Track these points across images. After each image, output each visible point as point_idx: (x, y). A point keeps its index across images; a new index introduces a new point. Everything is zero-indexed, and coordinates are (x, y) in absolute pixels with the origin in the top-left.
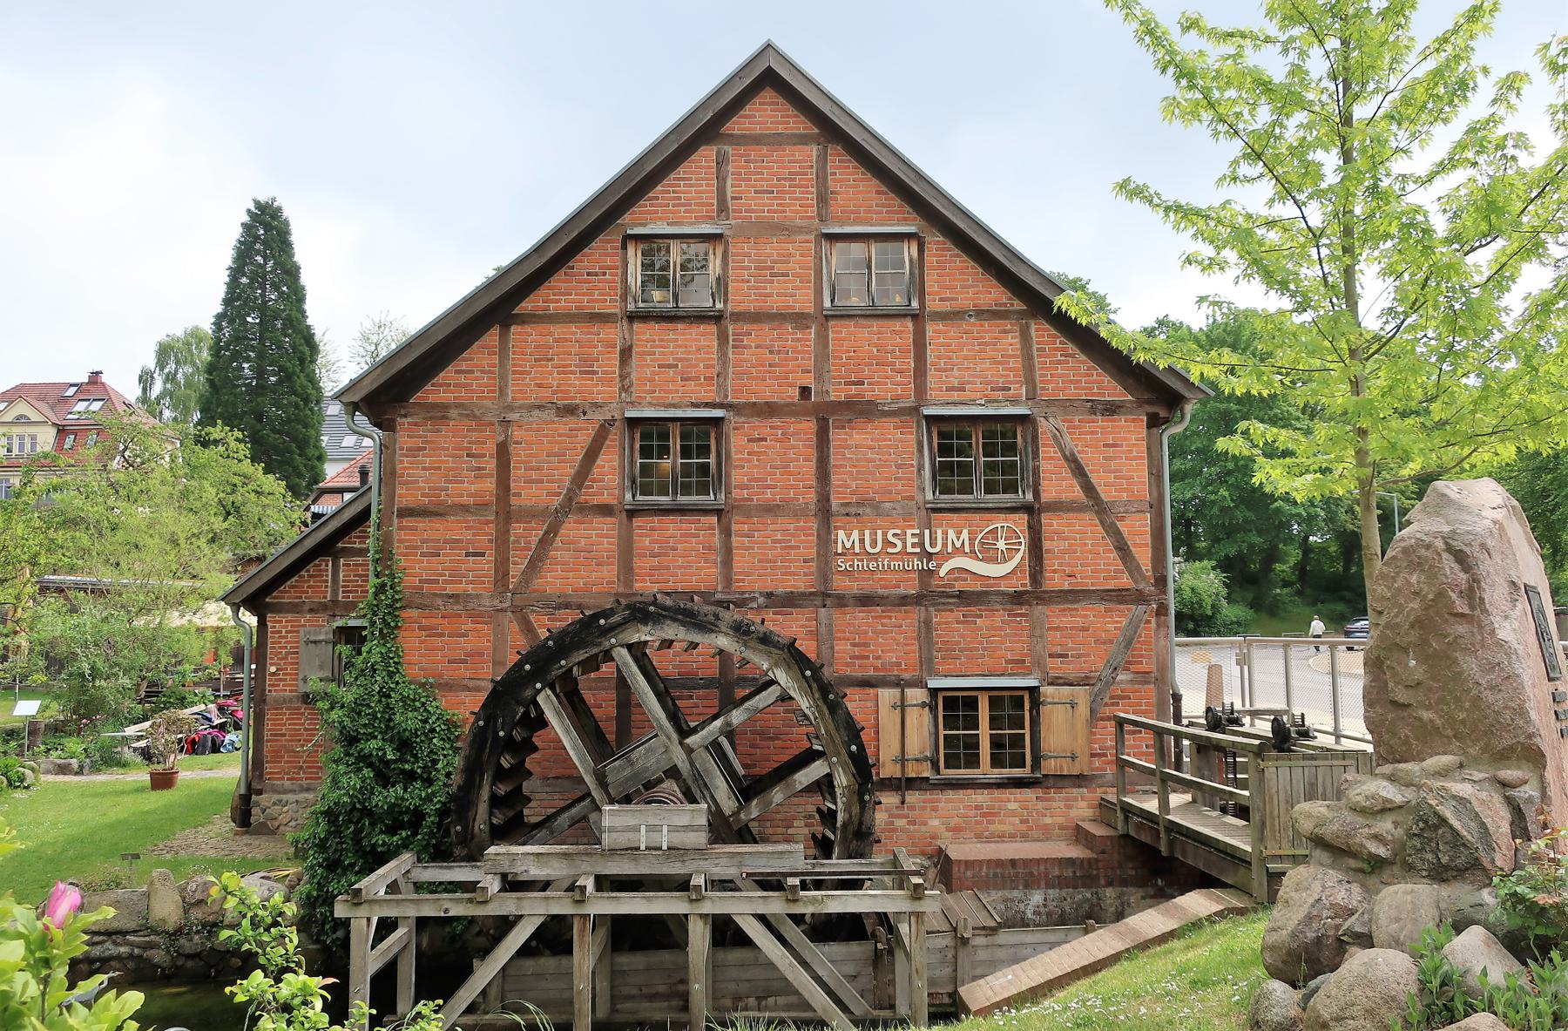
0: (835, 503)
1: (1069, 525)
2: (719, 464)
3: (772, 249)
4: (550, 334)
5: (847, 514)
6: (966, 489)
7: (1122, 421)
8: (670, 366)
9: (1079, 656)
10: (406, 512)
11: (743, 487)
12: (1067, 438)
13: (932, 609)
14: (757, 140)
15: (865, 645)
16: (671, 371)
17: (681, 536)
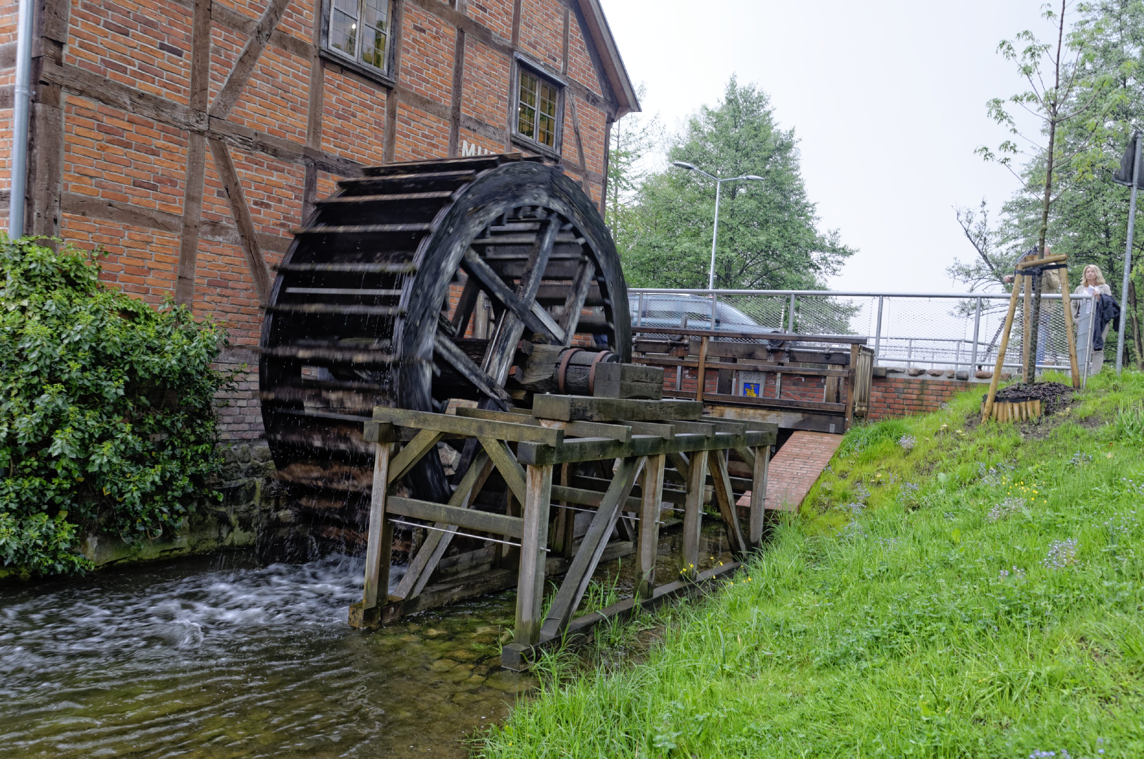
0: (462, 112)
5: (469, 128)
17: (362, 104)
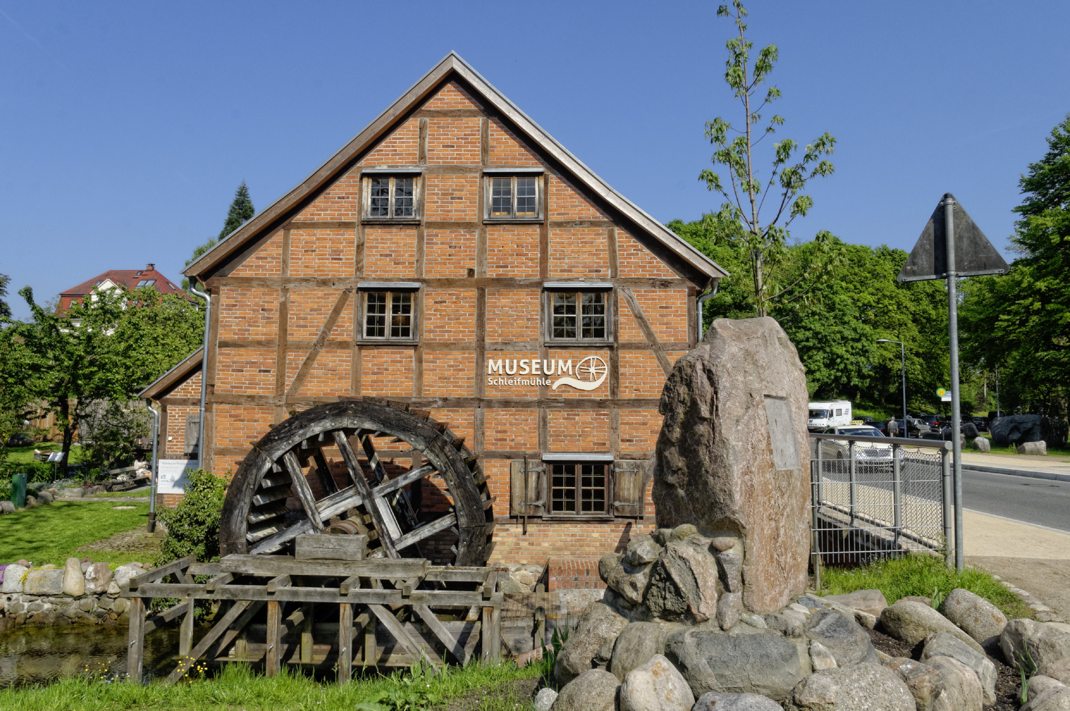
0: (488, 341)
1: (637, 358)
2: (415, 317)
3: (453, 181)
4: (314, 235)
6: (572, 334)
7: (671, 291)
8: (387, 255)
9: (641, 441)
10: (224, 344)
11: (430, 331)
12: (636, 302)
13: (548, 410)
14: (445, 114)
15: (505, 432)
16: (388, 259)
